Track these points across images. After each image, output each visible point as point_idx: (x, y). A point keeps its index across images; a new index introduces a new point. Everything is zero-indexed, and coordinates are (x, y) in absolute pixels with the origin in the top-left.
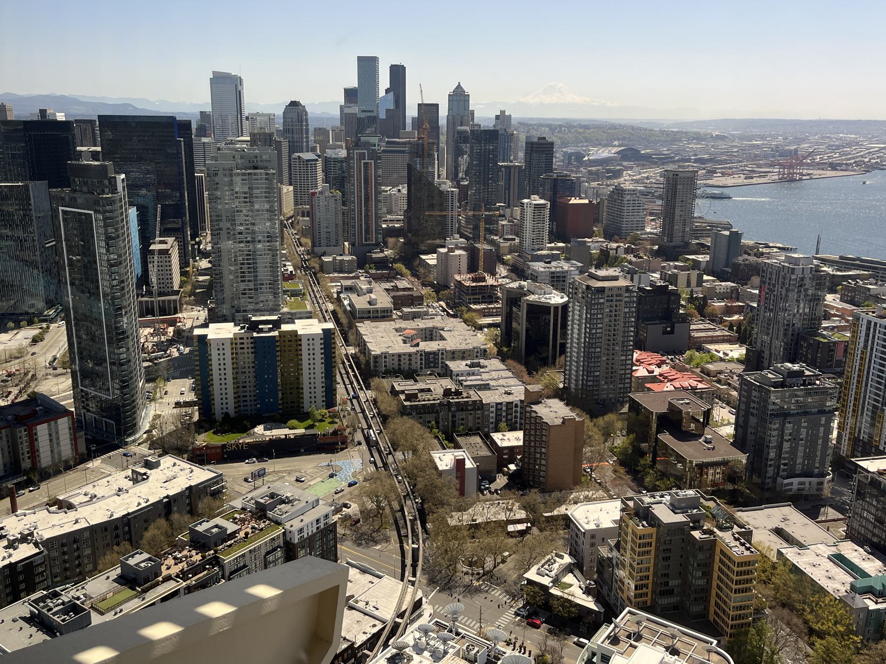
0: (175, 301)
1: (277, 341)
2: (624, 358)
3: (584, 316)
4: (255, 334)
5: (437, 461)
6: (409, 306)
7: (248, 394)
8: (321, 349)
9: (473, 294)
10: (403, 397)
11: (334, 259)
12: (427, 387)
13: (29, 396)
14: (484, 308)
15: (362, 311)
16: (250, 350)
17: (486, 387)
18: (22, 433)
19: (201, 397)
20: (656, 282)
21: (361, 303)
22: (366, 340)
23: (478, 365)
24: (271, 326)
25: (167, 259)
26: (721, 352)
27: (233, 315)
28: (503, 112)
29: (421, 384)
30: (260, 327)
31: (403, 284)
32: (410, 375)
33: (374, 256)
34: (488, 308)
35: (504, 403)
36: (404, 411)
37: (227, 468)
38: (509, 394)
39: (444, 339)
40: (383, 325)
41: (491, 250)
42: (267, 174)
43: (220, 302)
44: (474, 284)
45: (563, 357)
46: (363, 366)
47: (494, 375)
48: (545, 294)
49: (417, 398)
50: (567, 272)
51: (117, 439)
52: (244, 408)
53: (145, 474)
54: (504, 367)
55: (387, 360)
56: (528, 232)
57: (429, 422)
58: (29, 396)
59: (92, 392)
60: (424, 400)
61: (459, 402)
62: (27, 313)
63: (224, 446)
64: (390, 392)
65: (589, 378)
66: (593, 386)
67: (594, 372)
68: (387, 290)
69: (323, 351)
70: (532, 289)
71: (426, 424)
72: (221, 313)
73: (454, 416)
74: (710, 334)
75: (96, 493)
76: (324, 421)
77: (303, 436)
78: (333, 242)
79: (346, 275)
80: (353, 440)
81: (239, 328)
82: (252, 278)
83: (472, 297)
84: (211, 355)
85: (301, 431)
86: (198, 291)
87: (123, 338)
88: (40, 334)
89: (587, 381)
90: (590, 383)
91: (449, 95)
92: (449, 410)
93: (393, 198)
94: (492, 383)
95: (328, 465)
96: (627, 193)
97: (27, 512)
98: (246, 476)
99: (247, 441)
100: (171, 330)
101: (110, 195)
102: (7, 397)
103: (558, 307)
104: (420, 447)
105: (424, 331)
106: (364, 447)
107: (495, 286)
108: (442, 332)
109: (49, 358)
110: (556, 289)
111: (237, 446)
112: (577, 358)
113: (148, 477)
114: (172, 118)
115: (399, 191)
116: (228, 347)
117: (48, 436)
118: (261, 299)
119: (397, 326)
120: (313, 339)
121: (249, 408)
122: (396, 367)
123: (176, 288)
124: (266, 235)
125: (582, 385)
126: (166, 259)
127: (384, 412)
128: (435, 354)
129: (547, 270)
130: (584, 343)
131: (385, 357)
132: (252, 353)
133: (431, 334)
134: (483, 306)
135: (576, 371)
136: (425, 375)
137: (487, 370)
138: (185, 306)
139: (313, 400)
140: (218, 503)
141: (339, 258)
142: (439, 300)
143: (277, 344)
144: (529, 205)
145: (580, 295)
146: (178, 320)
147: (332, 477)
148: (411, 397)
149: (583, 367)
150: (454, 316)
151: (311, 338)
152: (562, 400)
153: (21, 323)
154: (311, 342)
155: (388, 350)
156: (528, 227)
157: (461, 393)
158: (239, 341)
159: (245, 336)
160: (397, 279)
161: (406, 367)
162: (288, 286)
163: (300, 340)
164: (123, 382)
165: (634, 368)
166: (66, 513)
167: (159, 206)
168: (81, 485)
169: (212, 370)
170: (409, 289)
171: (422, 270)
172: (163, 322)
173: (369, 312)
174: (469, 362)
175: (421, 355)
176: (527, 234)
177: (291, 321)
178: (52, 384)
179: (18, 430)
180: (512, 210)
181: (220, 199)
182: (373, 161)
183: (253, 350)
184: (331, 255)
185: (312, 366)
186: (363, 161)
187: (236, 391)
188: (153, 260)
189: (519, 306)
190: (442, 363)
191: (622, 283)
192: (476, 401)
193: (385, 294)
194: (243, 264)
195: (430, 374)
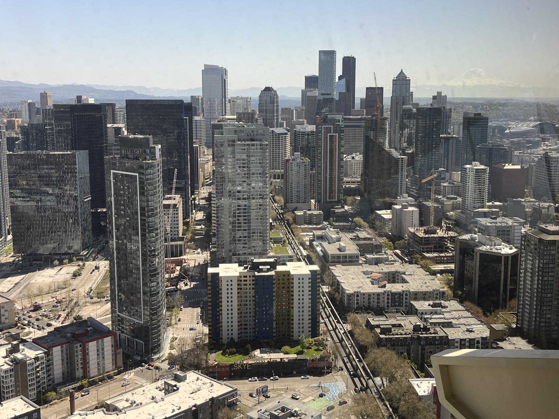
0: (181, 245)
1: (274, 280)
3: (537, 265)
4: (256, 274)
5: (416, 387)
6: (371, 253)
7: (248, 323)
8: (309, 287)
9: (425, 244)
10: (378, 331)
11: (305, 213)
12: (398, 322)
13: (75, 319)
14: (436, 257)
15: (333, 256)
16: (252, 286)
17: (449, 325)
18: (78, 347)
19: (211, 324)
21: (332, 249)
22: (340, 281)
23: (440, 305)
24: (269, 267)
27: (231, 257)
28: (439, 93)
29: (392, 320)
30: (260, 267)
31: (363, 234)
32: (379, 312)
33: (337, 211)
34: (439, 256)
35: (467, 340)
36: (380, 343)
37: (240, 384)
38: (471, 331)
39: (406, 282)
40: (352, 269)
41: (438, 207)
43: (220, 246)
44: (427, 236)
45: (514, 302)
46: (338, 303)
47: (455, 314)
48: (495, 246)
50: (511, 226)
51: (146, 356)
52: (246, 335)
53: (175, 386)
54: (462, 308)
55: (359, 298)
56: (470, 192)
57: (402, 353)
58: (75, 319)
59: (124, 315)
60: (397, 334)
61: (428, 337)
62: (66, 254)
63: (232, 365)
64: (366, 326)
65: (542, 320)
66: (545, 326)
67: (546, 314)
69: (310, 289)
70: (483, 241)
71: (400, 354)
72: (220, 257)
73: (423, 349)
75: (135, 400)
76: (311, 348)
77: (296, 359)
78: (302, 199)
79: (314, 226)
80: (335, 366)
81: (243, 268)
82: (247, 228)
83: (425, 247)
84: (221, 289)
85: (293, 356)
86: (197, 237)
87: (155, 275)
88: (79, 270)
89: (540, 322)
90: (543, 324)
91: (393, 80)
92: (419, 344)
93: (349, 164)
94: (454, 321)
95: (319, 387)
96: (554, 160)
97: (88, 412)
98: (251, 392)
99: (250, 362)
100: (178, 268)
101: (150, 161)
102: (58, 319)
104: (398, 375)
105: (387, 274)
106: (345, 372)
107: (445, 238)
108: (403, 276)
109: (87, 290)
110: (504, 241)
111: (242, 366)
112: (530, 302)
113: (178, 389)
114: (182, 101)
116: (235, 283)
117: (96, 351)
118: (253, 244)
119: (365, 270)
120: (303, 279)
121: (248, 335)
122: (367, 305)
123: (180, 235)
124: (259, 193)
125: (535, 325)
127: (362, 343)
128: (400, 294)
129: (494, 224)
130: (537, 289)
131: (357, 296)
132: (253, 288)
133: (393, 278)
134: (435, 255)
135: (529, 314)
136: (393, 313)
137: (448, 310)
138: (187, 250)
139: (301, 330)
140: (233, 413)
141: (308, 212)
142: (395, 248)
143: (274, 282)
144: (471, 170)
145: (532, 247)
146: (184, 261)
147: (322, 397)
148: (385, 331)
149: (536, 310)
150: (410, 263)
151: (301, 277)
153: (64, 261)
154: (301, 281)
155: (359, 290)
156: (470, 188)
157: (429, 329)
158: (243, 279)
159: (248, 275)
160: (357, 230)
161: (375, 305)
162: (272, 234)
163: (293, 279)
164: (153, 310)
166: (118, 415)
167: (176, 170)
168: (121, 392)
169: (221, 302)
170: (369, 239)
171: (378, 223)
172: (173, 262)
173: (339, 257)
174: (431, 303)
175: (388, 295)
176: (469, 194)
177: (285, 264)
178: (91, 309)
179: (75, 345)
180: (451, 174)
181: (224, 164)
182: (337, 134)
183: (254, 287)
184: (302, 210)
185: (301, 301)
186: (329, 134)
187: (239, 320)
188: (168, 212)
190: (406, 302)
192: (443, 337)
193: (351, 242)
194: (238, 216)
195: (397, 312)
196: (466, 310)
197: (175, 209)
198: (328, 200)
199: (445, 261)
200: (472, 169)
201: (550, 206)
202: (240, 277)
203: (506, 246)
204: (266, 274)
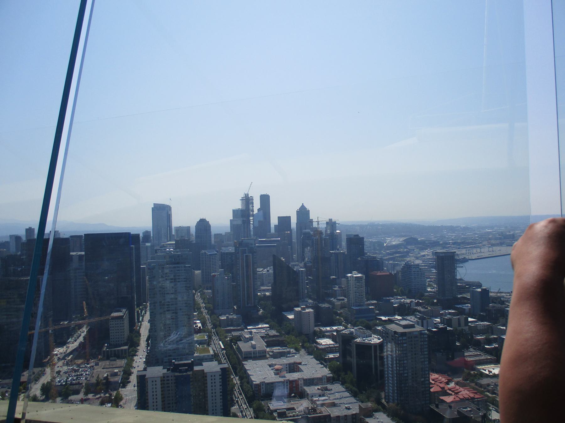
2: (423, 379)
4: (177, 374)
11: (227, 317)
12: (292, 406)
17: (334, 405)
20: (438, 325)
23: (326, 389)
25: (122, 322)
26: (487, 370)
28: (330, 220)
30: (180, 368)
41: (329, 307)
42: (185, 267)
47: (338, 396)
49: (286, 414)
68: (262, 337)
74: (477, 358)
96: (413, 267)
103: (376, 346)
105: (288, 365)
108: (300, 366)
114: (129, 234)
115: (268, 271)
116: (159, 383)
119: (270, 363)
126: (121, 322)
128: (296, 381)
133: (294, 368)
137: (332, 392)
143: (191, 380)
151: (213, 375)
152: (384, 413)
154: (213, 378)
163: (206, 377)
165: (431, 386)
173: (250, 353)
175: (287, 382)
182: (251, 254)
186: (245, 254)
189: (351, 345)
191: (418, 328)
196: (346, 391)
197: (122, 320)
198: (246, 305)
199: (335, 351)
200: (352, 277)
201: (411, 302)
202: (164, 377)
203: (375, 338)
204: (185, 374)
